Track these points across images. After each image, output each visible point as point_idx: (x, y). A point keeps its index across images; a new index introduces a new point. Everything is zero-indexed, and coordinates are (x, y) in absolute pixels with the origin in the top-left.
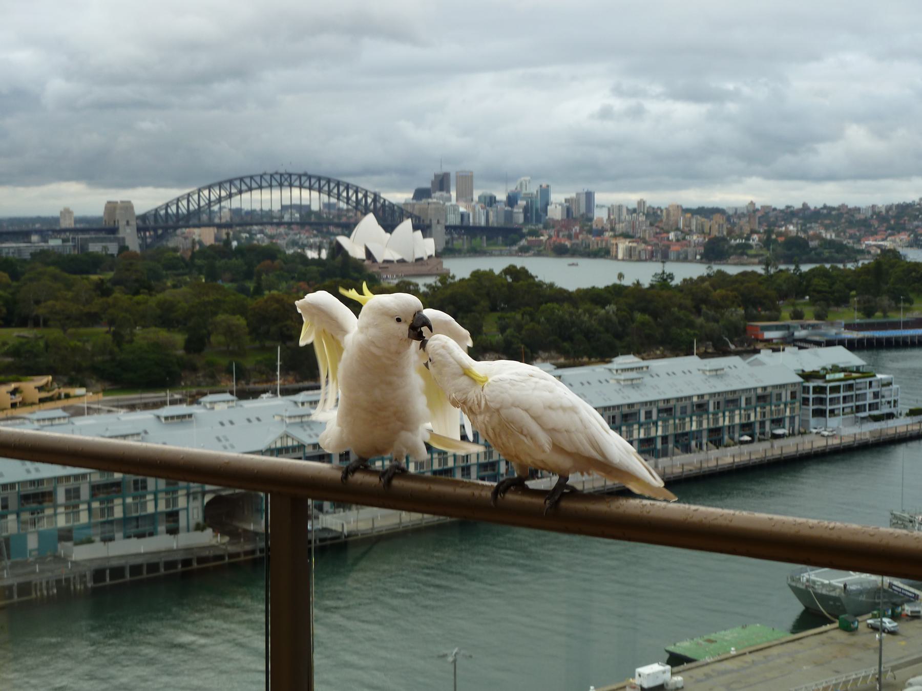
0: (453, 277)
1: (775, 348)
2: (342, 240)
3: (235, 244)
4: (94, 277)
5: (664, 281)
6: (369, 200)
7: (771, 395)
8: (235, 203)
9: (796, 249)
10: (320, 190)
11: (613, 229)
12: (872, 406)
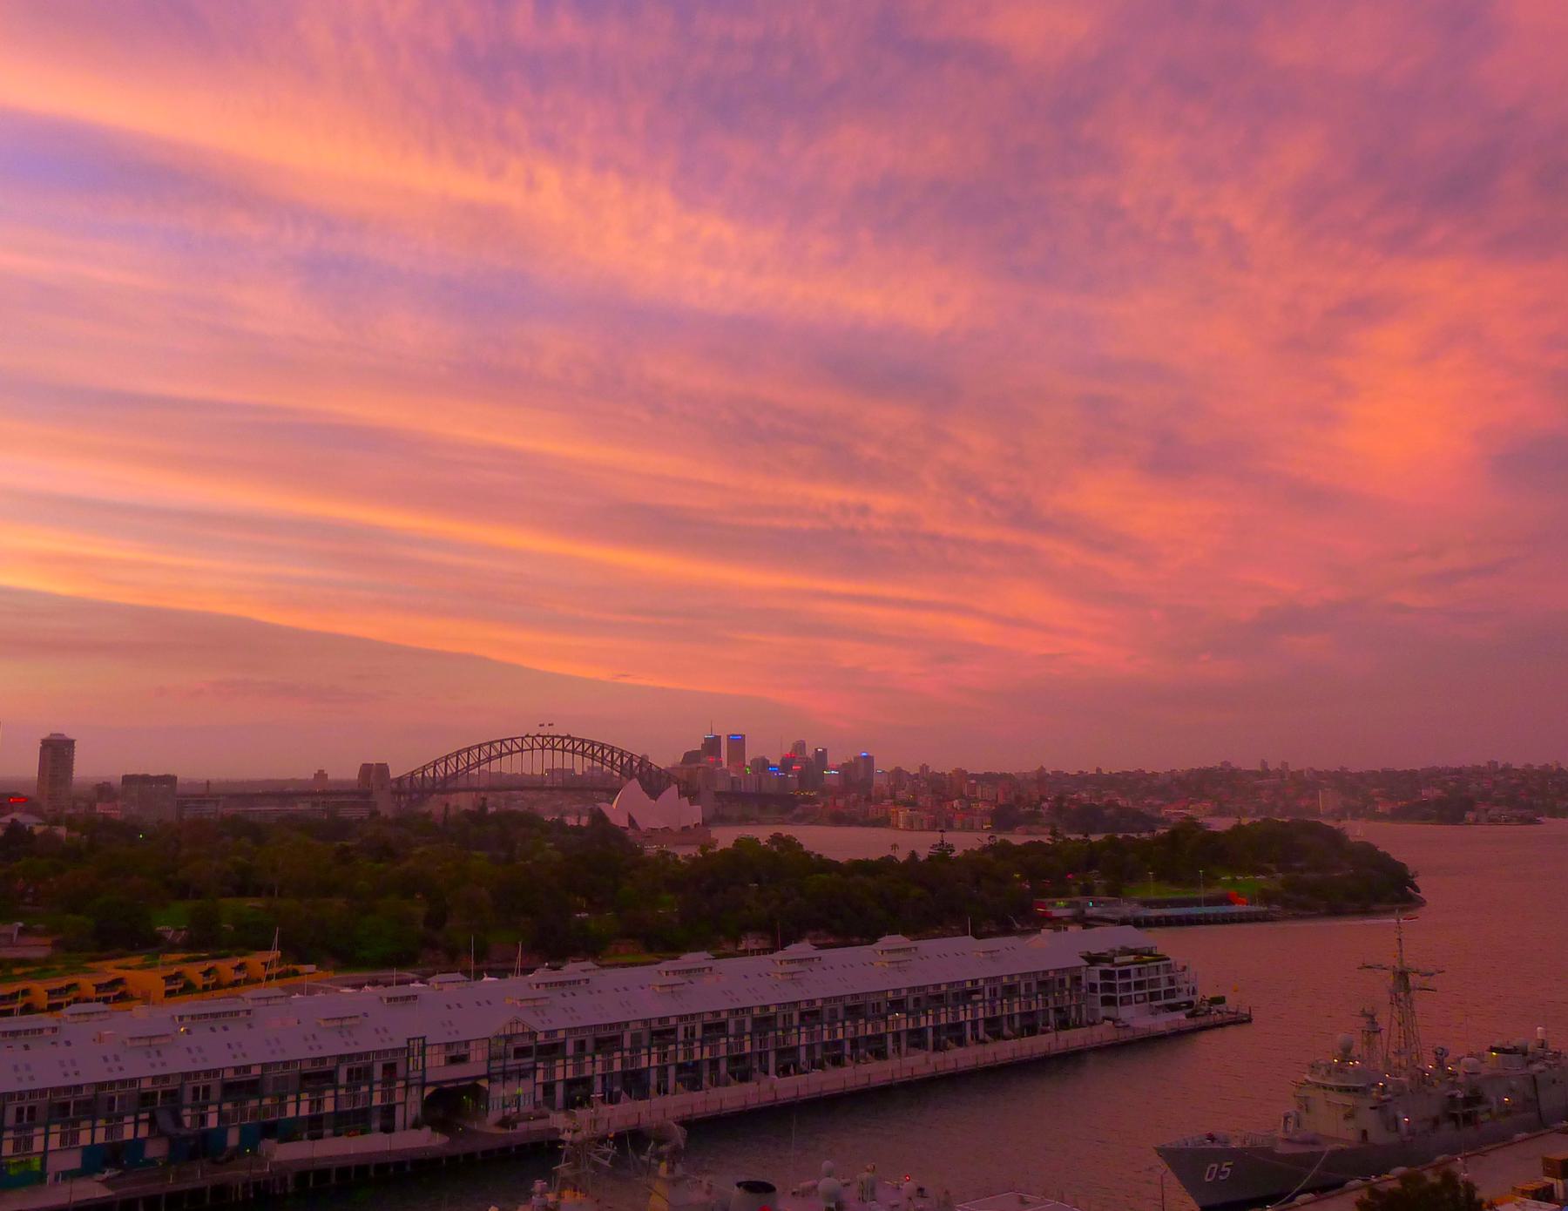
1: (1057, 923)
2: (603, 806)
4: (338, 844)
5: (943, 852)
7: (1053, 980)
8: (495, 766)
9: (1088, 817)
10: (583, 753)
11: (893, 796)
12: (1170, 993)
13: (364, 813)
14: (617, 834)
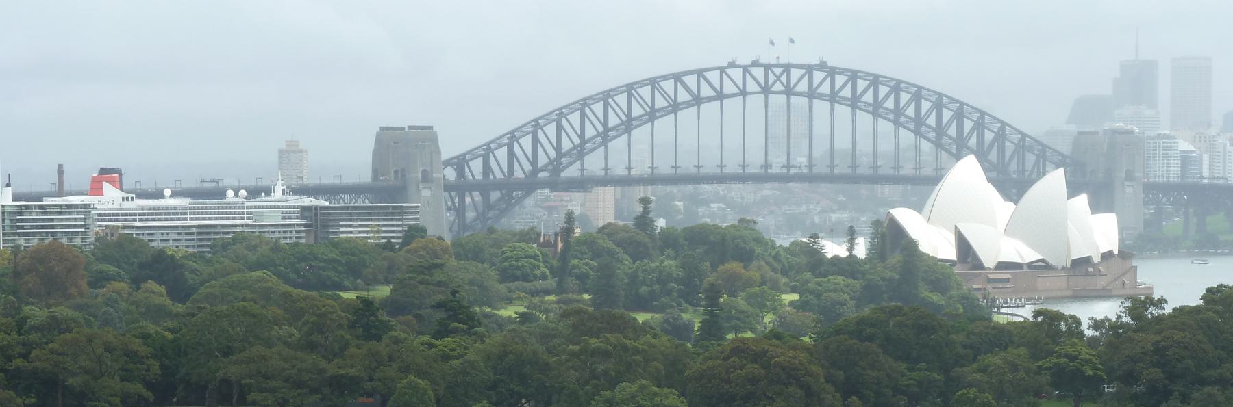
0: (1162, 301)
3: (661, 223)
6: (968, 125)
13: (393, 232)
14: (936, 272)
